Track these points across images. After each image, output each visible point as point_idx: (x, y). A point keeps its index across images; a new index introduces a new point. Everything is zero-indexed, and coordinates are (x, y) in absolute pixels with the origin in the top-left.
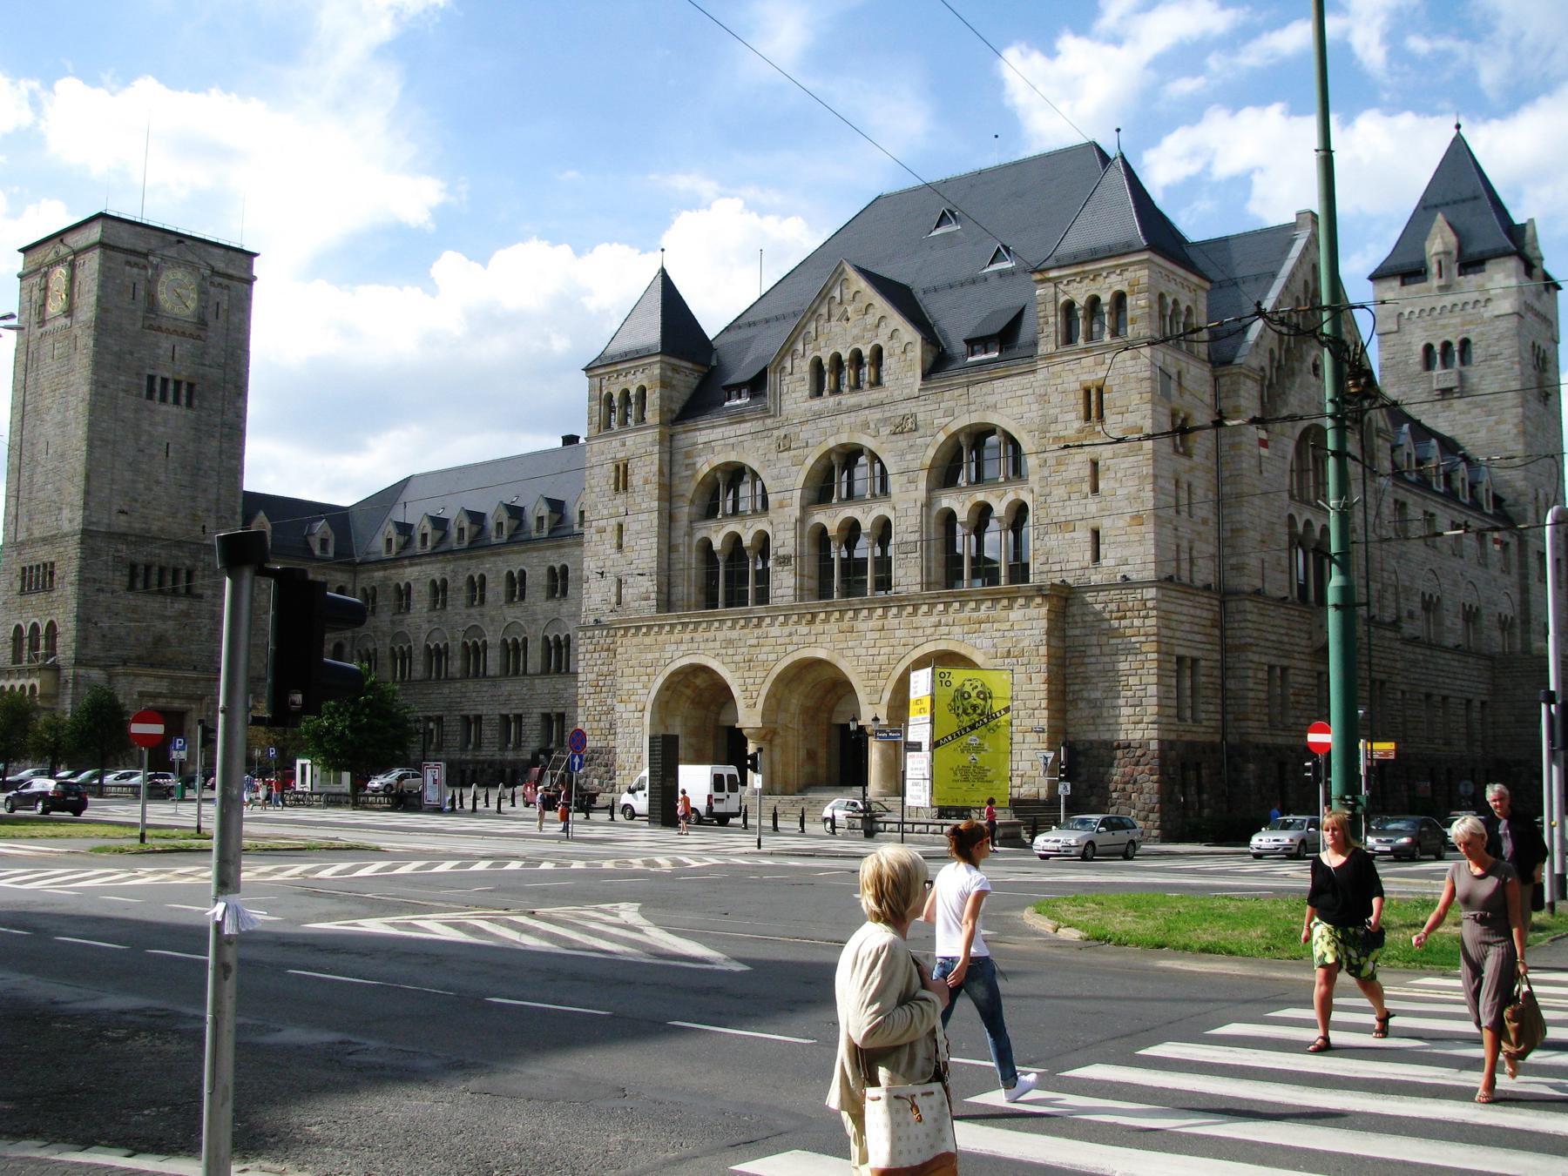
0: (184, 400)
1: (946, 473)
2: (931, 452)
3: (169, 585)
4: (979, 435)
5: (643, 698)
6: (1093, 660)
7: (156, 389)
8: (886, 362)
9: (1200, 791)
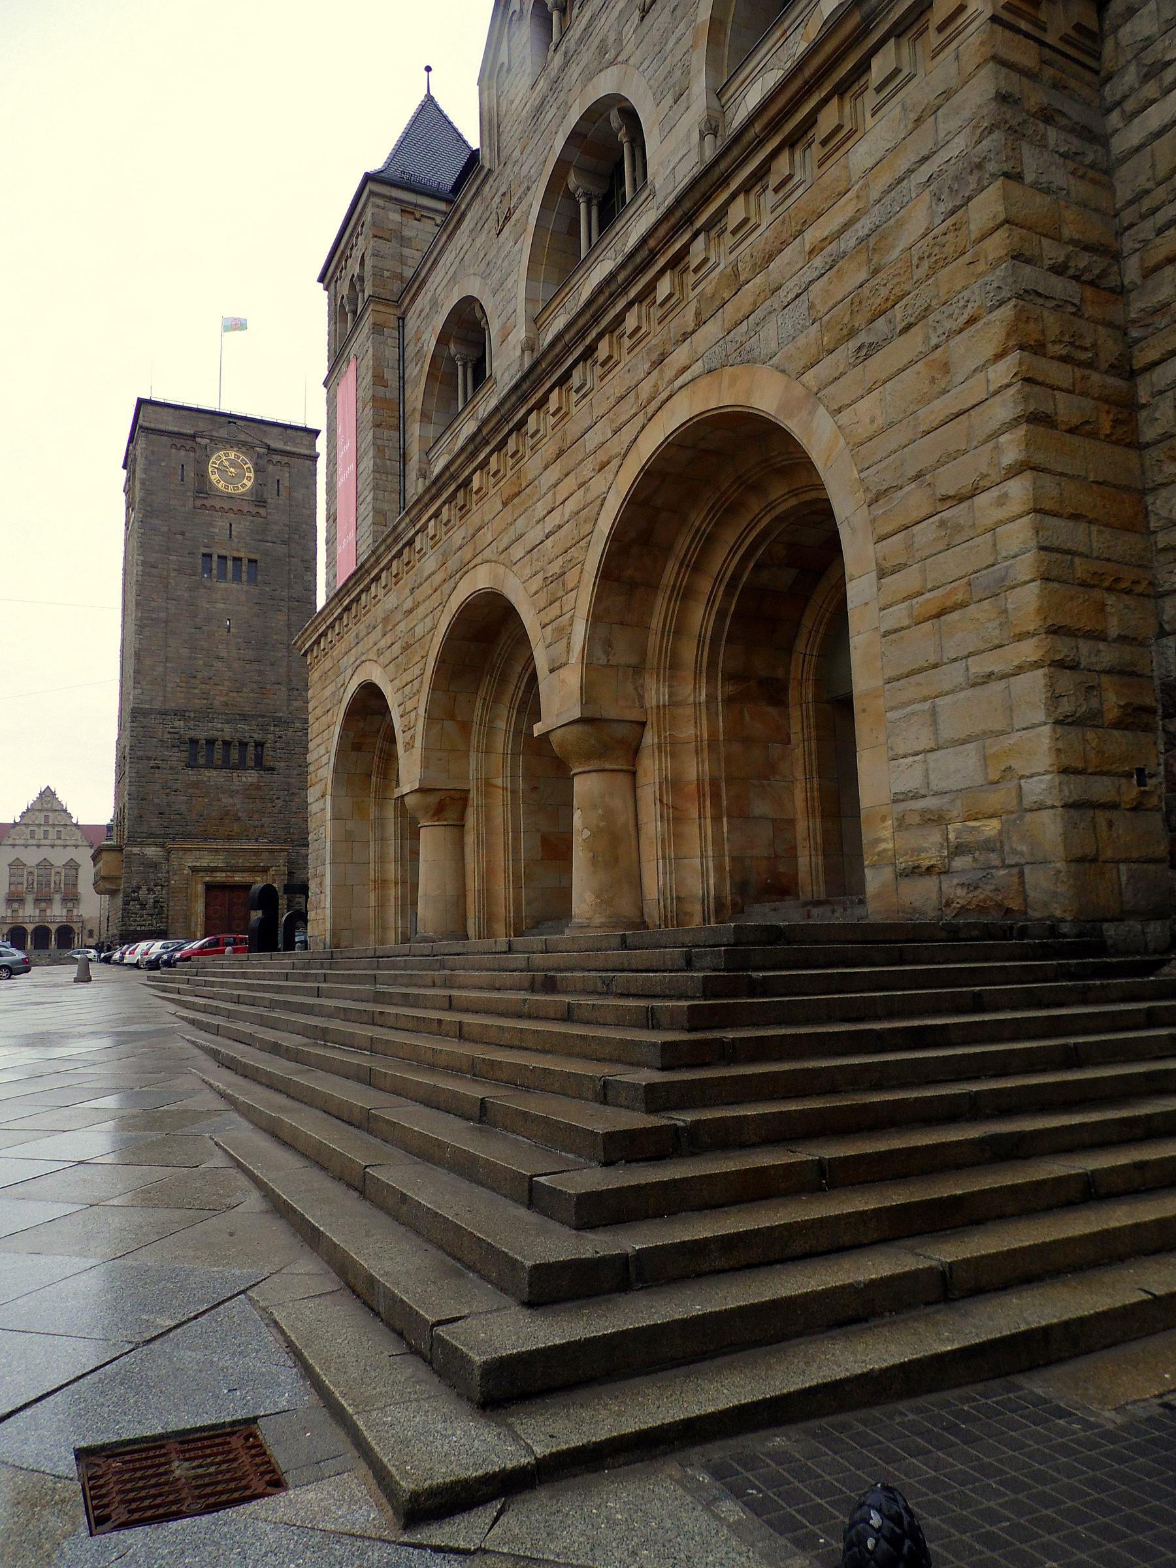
0: (244, 577)
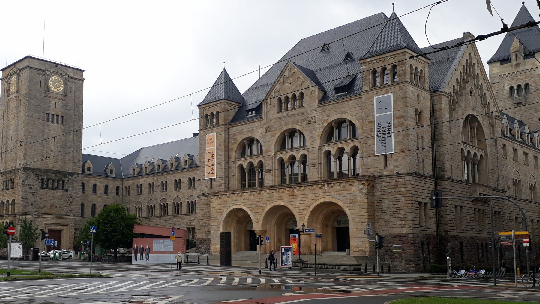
0: (60, 122)
1: (328, 136)
2: (322, 130)
3: (56, 185)
4: (340, 123)
5: (220, 221)
6: (385, 204)
7: (49, 117)
8: (305, 98)
9: (429, 254)
